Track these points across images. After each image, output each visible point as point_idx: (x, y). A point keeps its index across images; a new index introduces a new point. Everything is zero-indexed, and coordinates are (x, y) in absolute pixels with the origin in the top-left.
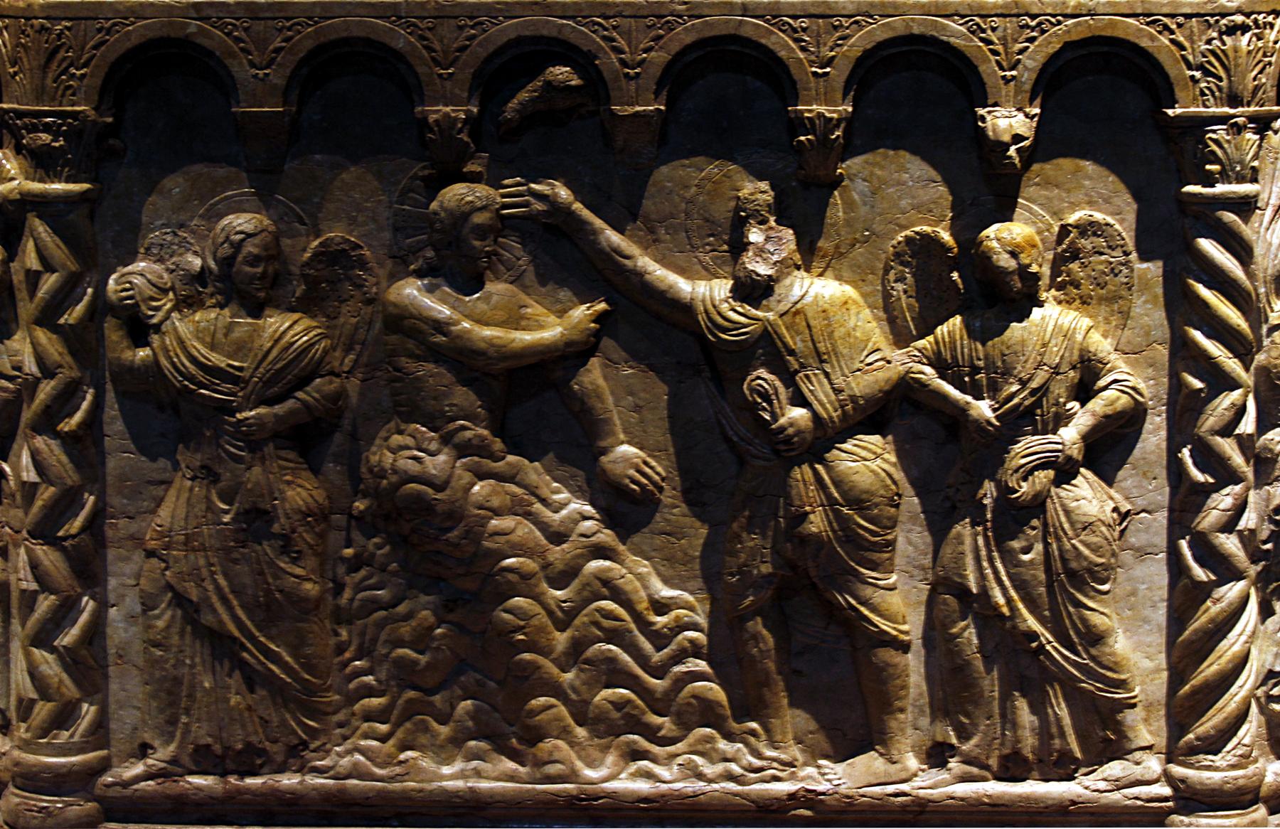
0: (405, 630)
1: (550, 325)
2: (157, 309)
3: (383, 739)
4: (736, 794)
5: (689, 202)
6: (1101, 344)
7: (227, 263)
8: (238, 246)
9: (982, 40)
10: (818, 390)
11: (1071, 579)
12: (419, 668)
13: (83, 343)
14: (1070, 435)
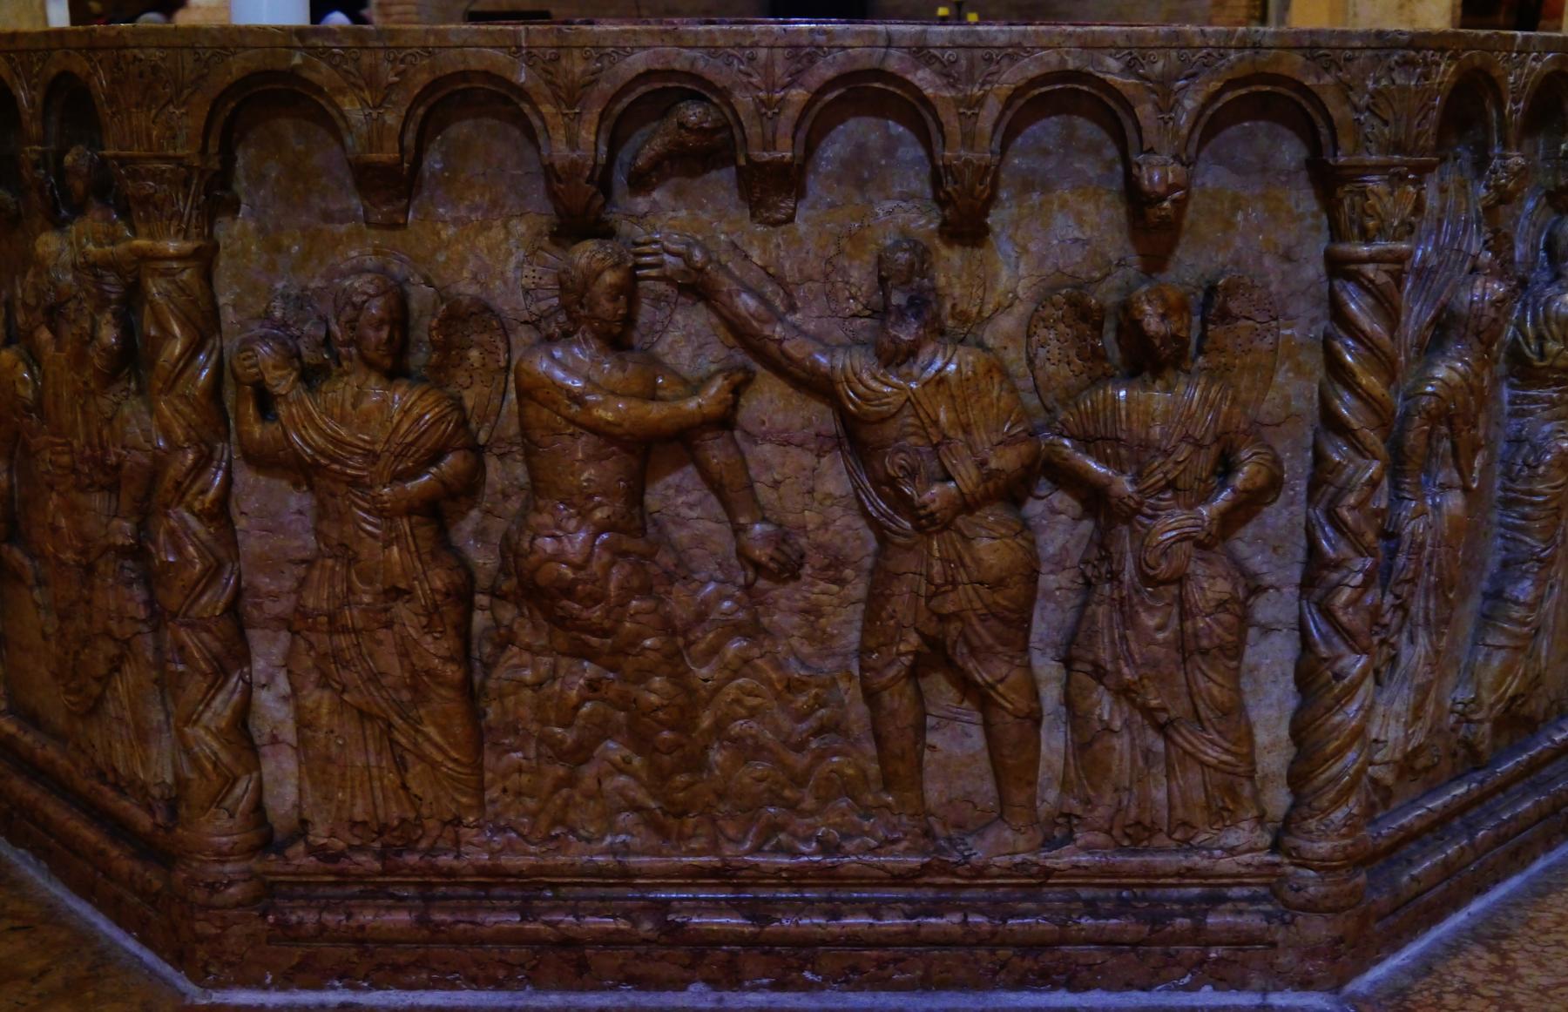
4: (870, 865)
12: (565, 747)
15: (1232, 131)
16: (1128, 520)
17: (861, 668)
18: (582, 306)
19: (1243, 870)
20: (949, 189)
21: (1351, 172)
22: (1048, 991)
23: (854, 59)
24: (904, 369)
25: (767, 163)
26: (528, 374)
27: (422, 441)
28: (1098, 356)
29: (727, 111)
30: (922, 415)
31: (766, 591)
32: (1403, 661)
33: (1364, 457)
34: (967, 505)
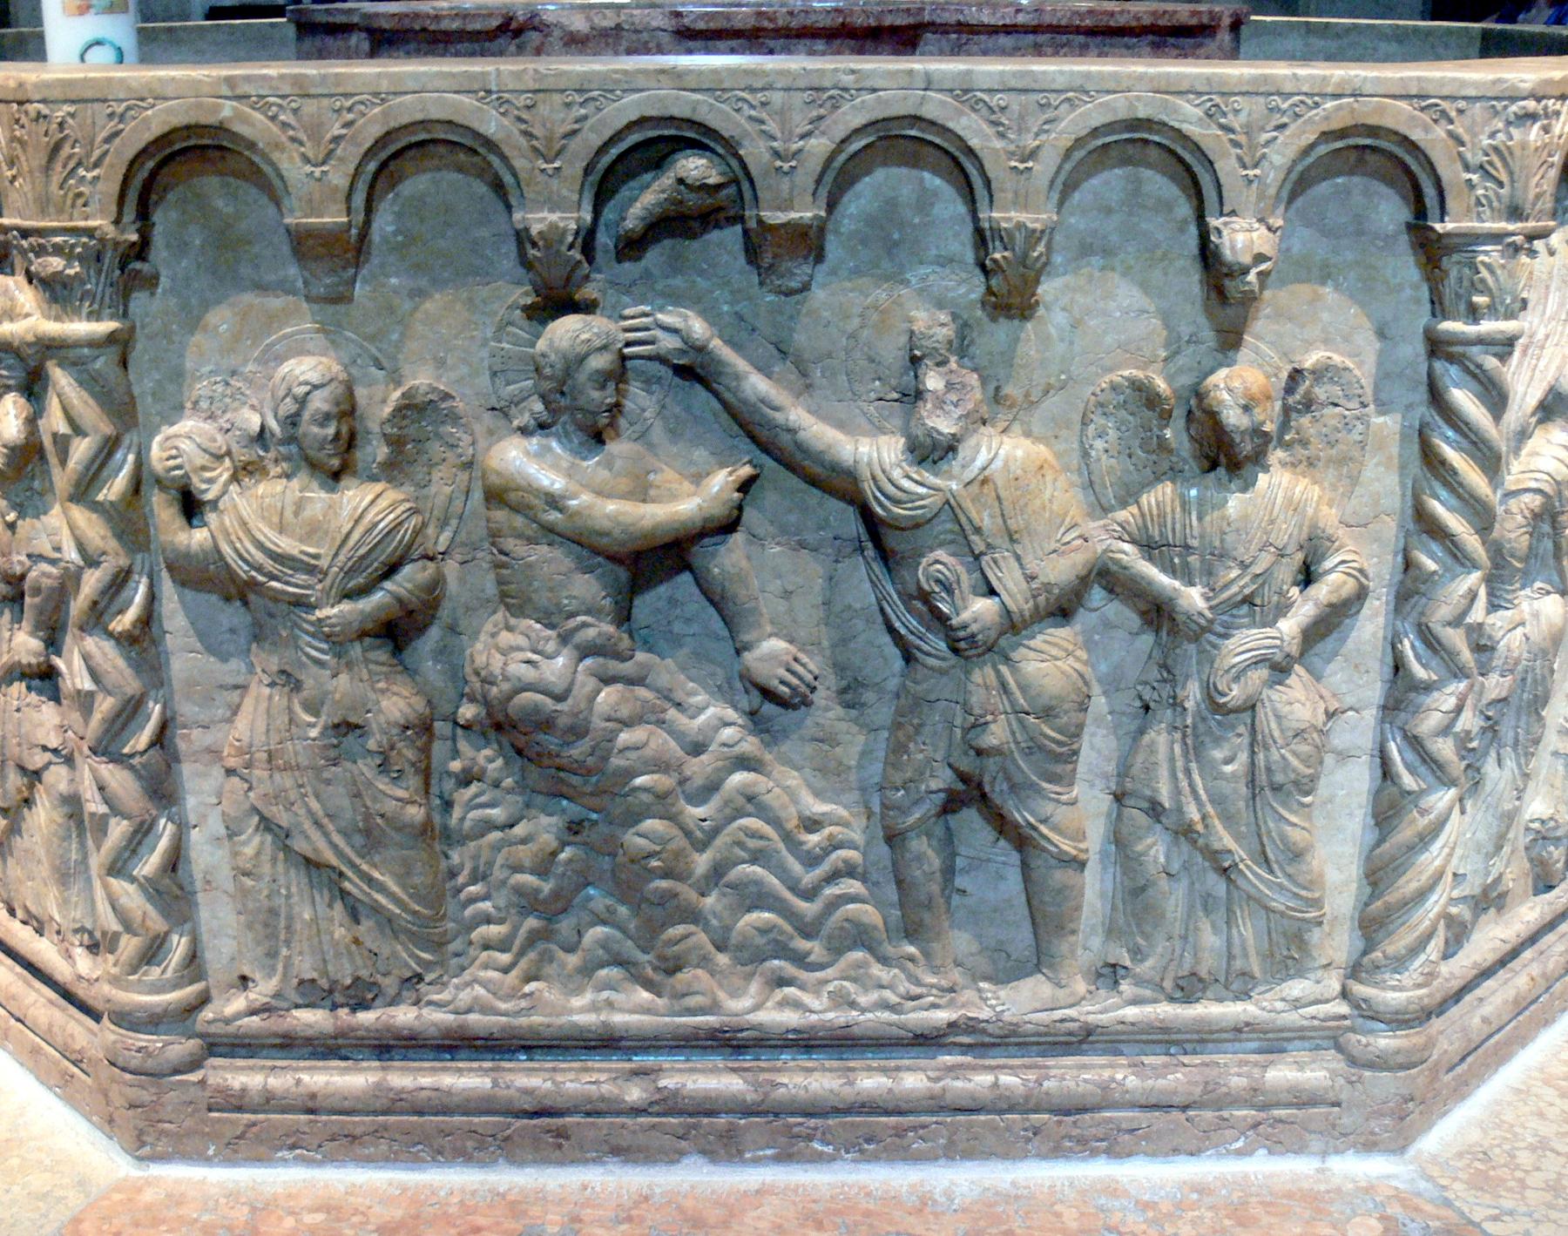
0: (524, 853)
1: (688, 493)
2: (211, 481)
3: (506, 970)
5: (852, 336)
6: (1329, 517)
7: (293, 421)
8: (302, 401)
9: (1223, 127)
10: (1009, 579)
11: (1273, 788)
12: (541, 896)
13: (129, 522)
14: (1289, 627)
15: (1324, 188)
16: (1196, 638)
17: (883, 805)
18: (563, 393)
19: (1305, 1023)
20: (997, 256)
21: (1456, 240)
22: (1084, 1159)
23: (886, 103)
24: (944, 466)
25: (783, 225)
26: (498, 474)
27: (374, 556)
28: (1163, 446)
29: (734, 163)
30: (963, 520)
31: (770, 719)
32: (1488, 787)
33: (1463, 565)
34: (1013, 625)
